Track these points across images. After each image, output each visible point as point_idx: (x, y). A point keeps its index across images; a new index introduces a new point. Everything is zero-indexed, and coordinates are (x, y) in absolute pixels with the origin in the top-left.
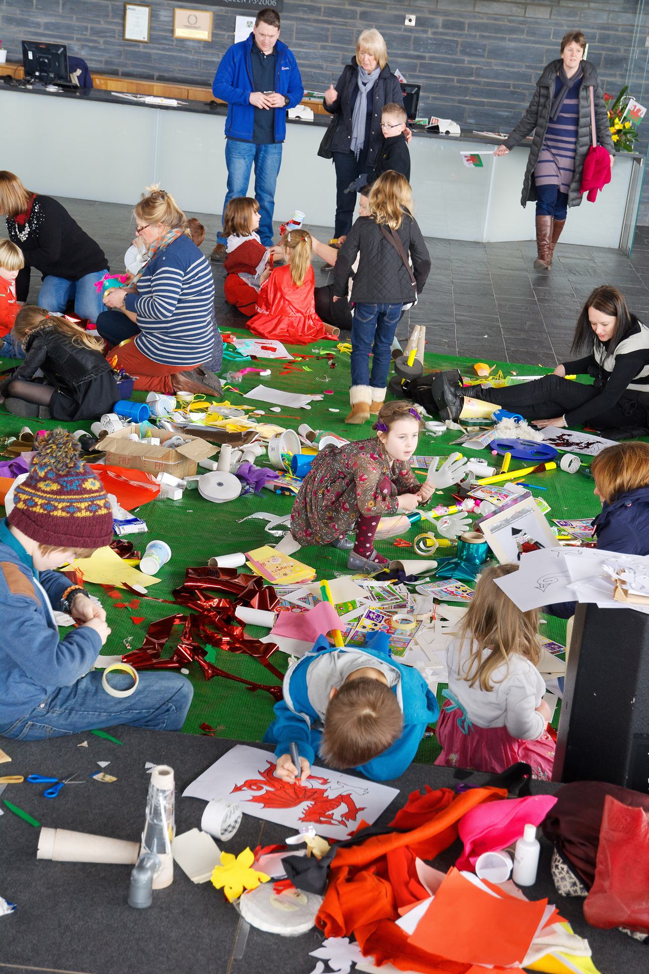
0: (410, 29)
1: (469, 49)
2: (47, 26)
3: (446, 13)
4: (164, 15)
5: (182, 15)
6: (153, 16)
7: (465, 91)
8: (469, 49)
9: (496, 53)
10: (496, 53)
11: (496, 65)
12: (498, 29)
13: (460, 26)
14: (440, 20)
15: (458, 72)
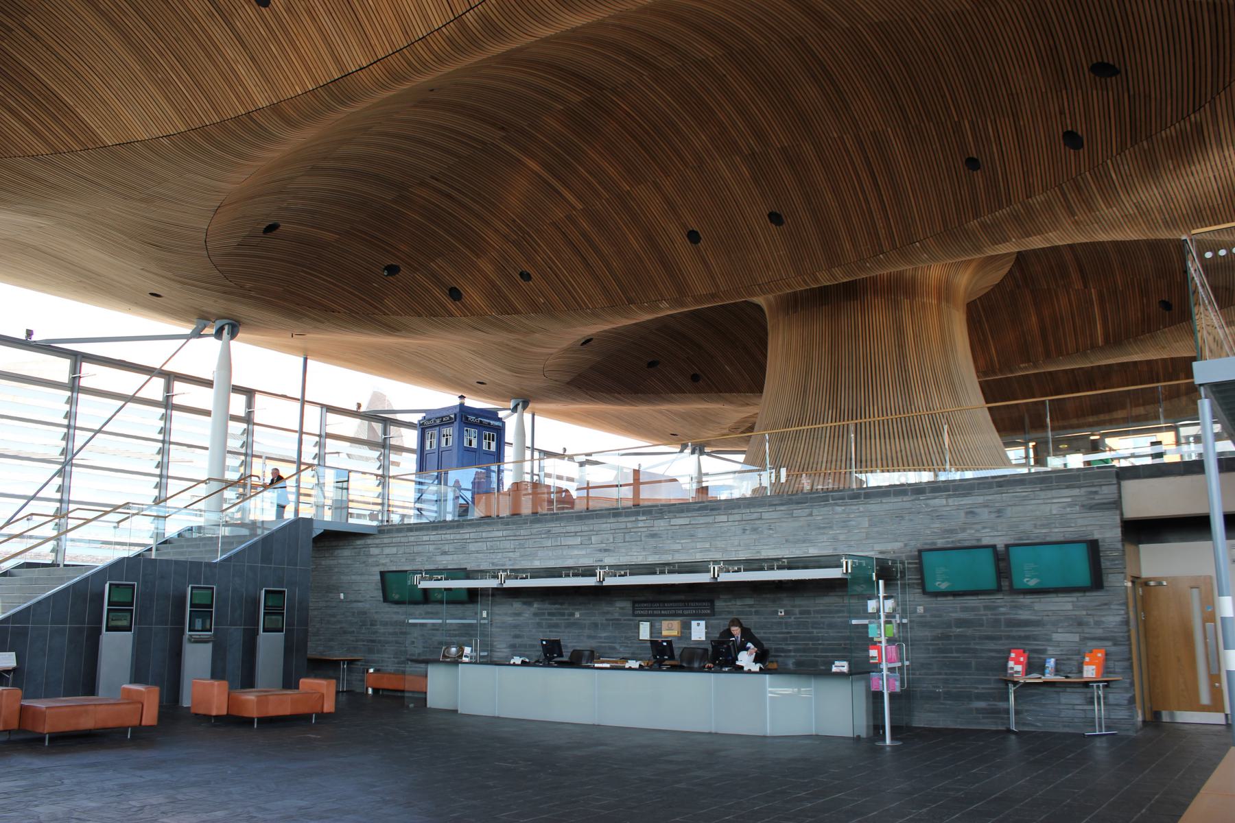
0: (781, 617)
1: (815, 625)
2: (606, 638)
3: (800, 606)
4: (657, 624)
5: (665, 624)
6: (652, 626)
7: (816, 650)
8: (815, 625)
9: (831, 626)
10: (831, 626)
11: (832, 633)
12: (830, 612)
13: (808, 612)
14: (797, 610)
15: (811, 639)
